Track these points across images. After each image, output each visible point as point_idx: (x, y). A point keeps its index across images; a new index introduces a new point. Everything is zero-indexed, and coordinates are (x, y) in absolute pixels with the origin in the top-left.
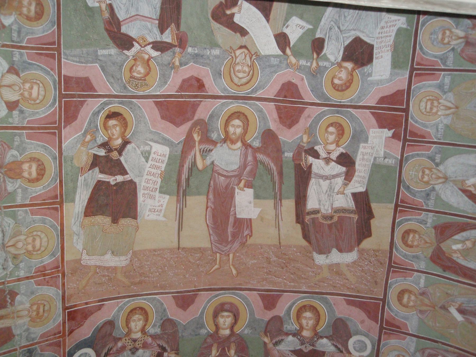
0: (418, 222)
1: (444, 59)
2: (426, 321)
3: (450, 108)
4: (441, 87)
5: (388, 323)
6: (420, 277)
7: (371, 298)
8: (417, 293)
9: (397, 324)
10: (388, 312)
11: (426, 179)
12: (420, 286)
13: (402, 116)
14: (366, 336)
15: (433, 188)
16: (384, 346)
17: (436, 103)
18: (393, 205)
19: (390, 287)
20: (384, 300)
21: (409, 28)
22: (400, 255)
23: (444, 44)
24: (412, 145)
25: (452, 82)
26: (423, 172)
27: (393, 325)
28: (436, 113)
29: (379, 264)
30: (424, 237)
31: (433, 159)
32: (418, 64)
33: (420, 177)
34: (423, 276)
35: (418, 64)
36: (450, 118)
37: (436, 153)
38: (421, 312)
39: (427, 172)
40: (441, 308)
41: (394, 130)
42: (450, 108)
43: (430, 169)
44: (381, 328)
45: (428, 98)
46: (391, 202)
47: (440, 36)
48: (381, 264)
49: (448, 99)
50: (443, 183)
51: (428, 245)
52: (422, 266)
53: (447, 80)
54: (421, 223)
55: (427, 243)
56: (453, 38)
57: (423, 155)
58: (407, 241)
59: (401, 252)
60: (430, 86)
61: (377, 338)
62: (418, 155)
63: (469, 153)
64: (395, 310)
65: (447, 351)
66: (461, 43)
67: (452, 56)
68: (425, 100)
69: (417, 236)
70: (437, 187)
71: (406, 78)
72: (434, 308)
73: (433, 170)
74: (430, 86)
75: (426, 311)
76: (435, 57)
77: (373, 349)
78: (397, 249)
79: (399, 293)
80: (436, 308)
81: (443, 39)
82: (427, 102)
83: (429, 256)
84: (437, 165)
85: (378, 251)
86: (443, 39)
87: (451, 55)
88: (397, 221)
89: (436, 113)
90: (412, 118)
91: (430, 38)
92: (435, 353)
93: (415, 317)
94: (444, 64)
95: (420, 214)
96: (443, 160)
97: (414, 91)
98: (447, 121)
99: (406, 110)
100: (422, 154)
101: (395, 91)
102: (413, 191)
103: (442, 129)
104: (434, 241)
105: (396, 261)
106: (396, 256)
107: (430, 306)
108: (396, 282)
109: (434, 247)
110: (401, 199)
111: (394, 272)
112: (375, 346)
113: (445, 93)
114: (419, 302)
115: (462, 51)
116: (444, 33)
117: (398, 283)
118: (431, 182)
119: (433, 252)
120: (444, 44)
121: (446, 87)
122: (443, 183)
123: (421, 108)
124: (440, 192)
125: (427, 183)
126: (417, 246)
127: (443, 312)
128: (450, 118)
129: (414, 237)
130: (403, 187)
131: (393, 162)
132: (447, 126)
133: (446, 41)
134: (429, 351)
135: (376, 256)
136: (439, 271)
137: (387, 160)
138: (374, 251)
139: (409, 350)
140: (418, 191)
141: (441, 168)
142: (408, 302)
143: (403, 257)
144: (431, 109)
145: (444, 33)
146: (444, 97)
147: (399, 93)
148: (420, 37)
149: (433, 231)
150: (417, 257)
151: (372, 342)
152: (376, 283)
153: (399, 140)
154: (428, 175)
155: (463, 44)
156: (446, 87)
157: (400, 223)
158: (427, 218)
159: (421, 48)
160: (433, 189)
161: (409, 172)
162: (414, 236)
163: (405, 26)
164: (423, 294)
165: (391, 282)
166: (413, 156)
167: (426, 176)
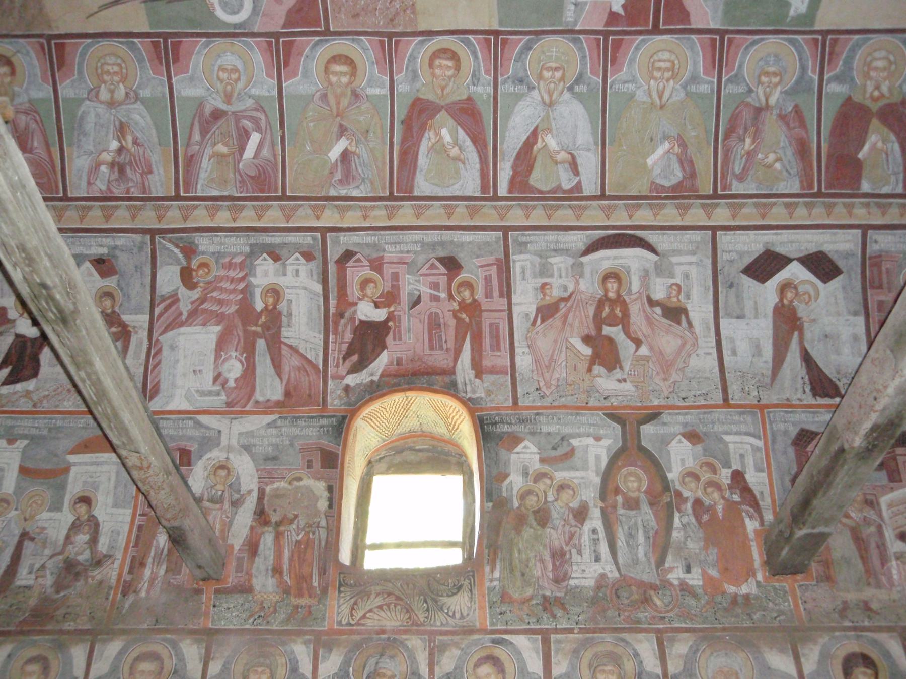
0: (474, 71)
1: (737, 79)
2: (311, 106)
3: (661, 97)
4: (694, 79)
5: (289, 45)
6: (382, 86)
7: (326, 10)
8: (354, 85)
9: (292, 60)
10: (308, 42)
11: (547, 74)
12: (368, 89)
13: (647, 24)
14: (255, 11)
15: (534, 88)
16: (246, 44)
17: (668, 75)
18: (496, 26)
19: (353, 40)
20: (327, 32)
21: (789, 19)
22: (413, 50)
23: (759, 77)
24: (599, 45)
25: (702, 96)
26: (556, 69)
27: (288, 55)
28: (653, 78)
29: (390, 16)
30: (451, 84)
31: (579, 80)
32: (730, 41)
33: (548, 65)
34: (386, 91)
35: (730, 41)
36: (646, 99)
37: (589, 85)
38: (324, 97)
39: (558, 75)
40: (341, 126)
41: (623, 13)
42: (661, 97)
43: (562, 79)
44: (277, 35)
45: (676, 62)
46: (501, 23)
47: (771, 69)
48: (392, 20)
49: (674, 92)
50: (544, 103)
51: (439, 91)
52: (402, 87)
53: (704, 88)
54: (474, 76)
55: (443, 90)
56: (768, 89)
57: (584, 65)
58: (440, 58)
59: (417, 52)
60: (695, 64)
61: (256, 31)
62: (584, 57)
63: (594, 133)
64: (314, 55)
65: (273, 145)
66: (759, 100)
67: (741, 90)
68: (673, 57)
69: (450, 73)
70: (535, 93)
71: (709, 24)
72: (338, 115)
73: (562, 83)
74: (695, 64)
75: (329, 105)
76: (740, 66)
77: (235, 26)
78: (422, 43)
79: (347, 57)
80: (339, 118)
81: (767, 74)
82: (669, 61)
83: (421, 96)
84: (571, 89)
85: (414, 12)
86: (767, 74)
87: (742, 89)
88: (470, 37)
89: (653, 78)
90: (643, 40)
91: (769, 55)
92: (263, 128)
93: (314, 88)
94: (729, 81)
95: (487, 72)
96: (579, 97)
97: (689, 39)
98: (641, 95)
99: (656, 30)
100: (586, 64)
101: (688, 9)
102: (524, 56)
103: (628, 88)
104: (448, 101)
105: (401, 45)
106: (409, 43)
107: (338, 108)
108: (365, 50)
109: (437, 101)
110: (507, 39)
111: (382, 43)
112: (239, 28)
113: (684, 87)
114: (339, 90)
115: (748, 105)
116: (775, 74)
117: (364, 52)
118: (541, 83)
119: (428, 101)
120: (759, 77)
121: (693, 88)
122: (544, 103)
123: (660, 54)
124: (528, 99)
125: (540, 77)
126: (433, 75)
127: (335, 129)
128: (646, 99)
129: (448, 67)
130: (529, 40)
131: (569, 19)
132: (632, 96)
133: (764, 79)
134: (263, 117)
135: (405, 11)
136: (401, 113)
137: (572, 7)
138: (413, 5)
139: (252, 87)
140: (525, 65)
141: (567, 95)
142: (335, 74)
143: (411, 56)
144: (659, 69)
145: (775, 74)
146: (678, 86)
147: (685, 16)
148: (772, 38)
149: (465, 97)
150: (415, 76)
151: (245, 22)
152: (357, 15)
153: (608, 24)
154: (553, 77)
155: (757, 105)
156: (693, 88)
157: (468, 43)
158: (483, 85)
159: (754, 43)
160: (531, 88)
161: (554, 48)
162: (448, 67)
163: (792, 12)
164: (356, 95)
165: (362, 40)
166: (581, 49)
167: (550, 73)
